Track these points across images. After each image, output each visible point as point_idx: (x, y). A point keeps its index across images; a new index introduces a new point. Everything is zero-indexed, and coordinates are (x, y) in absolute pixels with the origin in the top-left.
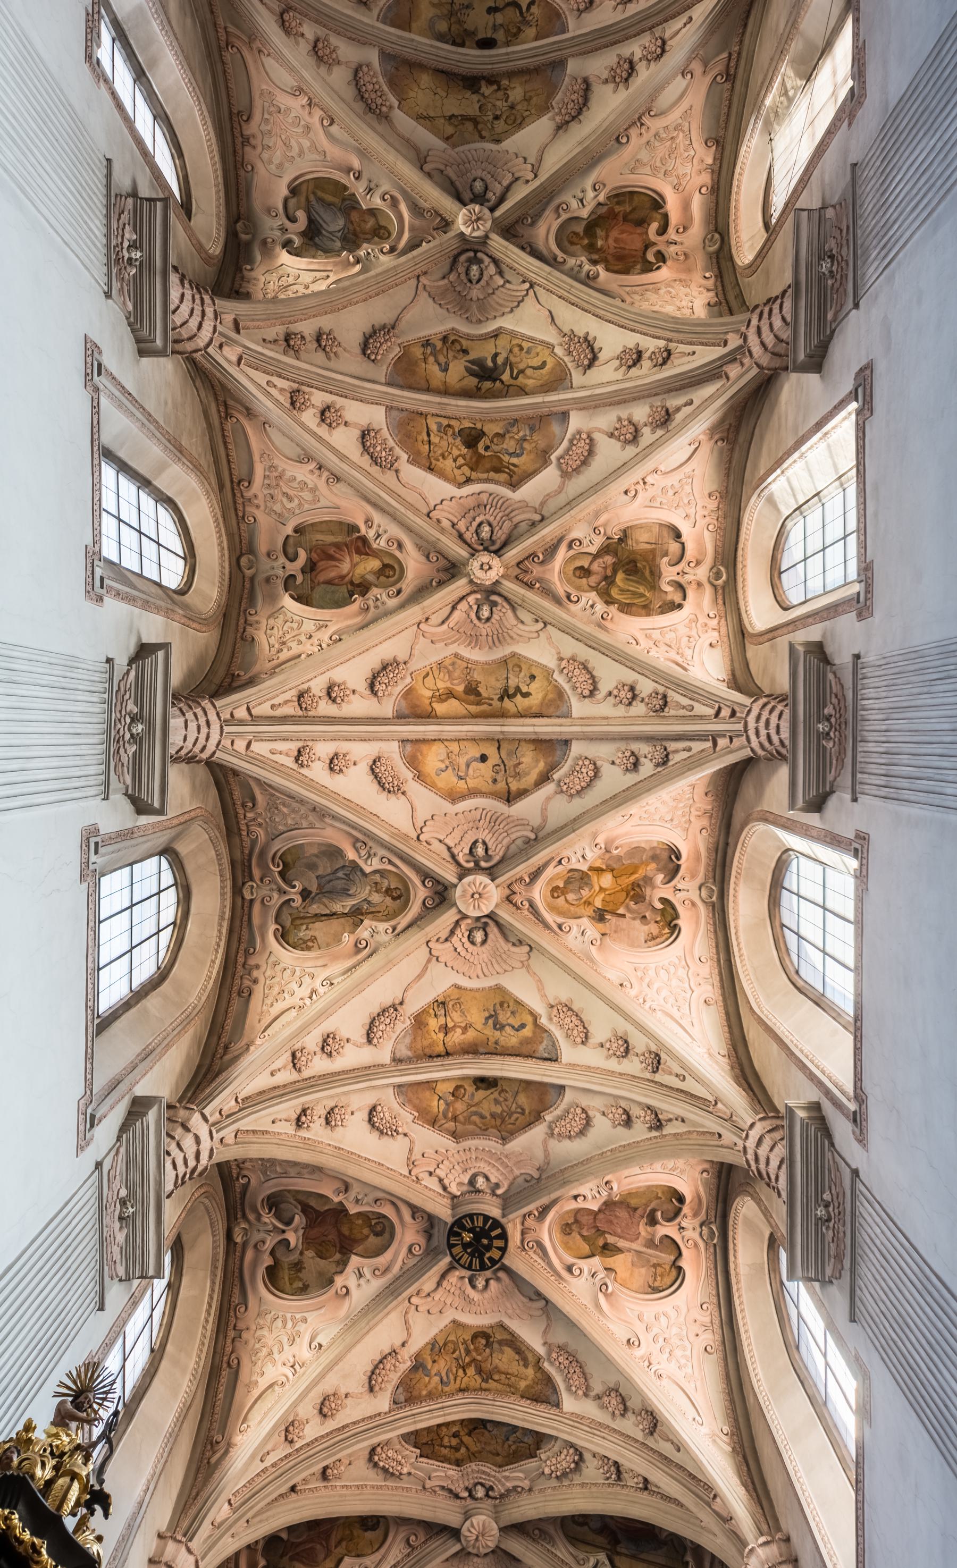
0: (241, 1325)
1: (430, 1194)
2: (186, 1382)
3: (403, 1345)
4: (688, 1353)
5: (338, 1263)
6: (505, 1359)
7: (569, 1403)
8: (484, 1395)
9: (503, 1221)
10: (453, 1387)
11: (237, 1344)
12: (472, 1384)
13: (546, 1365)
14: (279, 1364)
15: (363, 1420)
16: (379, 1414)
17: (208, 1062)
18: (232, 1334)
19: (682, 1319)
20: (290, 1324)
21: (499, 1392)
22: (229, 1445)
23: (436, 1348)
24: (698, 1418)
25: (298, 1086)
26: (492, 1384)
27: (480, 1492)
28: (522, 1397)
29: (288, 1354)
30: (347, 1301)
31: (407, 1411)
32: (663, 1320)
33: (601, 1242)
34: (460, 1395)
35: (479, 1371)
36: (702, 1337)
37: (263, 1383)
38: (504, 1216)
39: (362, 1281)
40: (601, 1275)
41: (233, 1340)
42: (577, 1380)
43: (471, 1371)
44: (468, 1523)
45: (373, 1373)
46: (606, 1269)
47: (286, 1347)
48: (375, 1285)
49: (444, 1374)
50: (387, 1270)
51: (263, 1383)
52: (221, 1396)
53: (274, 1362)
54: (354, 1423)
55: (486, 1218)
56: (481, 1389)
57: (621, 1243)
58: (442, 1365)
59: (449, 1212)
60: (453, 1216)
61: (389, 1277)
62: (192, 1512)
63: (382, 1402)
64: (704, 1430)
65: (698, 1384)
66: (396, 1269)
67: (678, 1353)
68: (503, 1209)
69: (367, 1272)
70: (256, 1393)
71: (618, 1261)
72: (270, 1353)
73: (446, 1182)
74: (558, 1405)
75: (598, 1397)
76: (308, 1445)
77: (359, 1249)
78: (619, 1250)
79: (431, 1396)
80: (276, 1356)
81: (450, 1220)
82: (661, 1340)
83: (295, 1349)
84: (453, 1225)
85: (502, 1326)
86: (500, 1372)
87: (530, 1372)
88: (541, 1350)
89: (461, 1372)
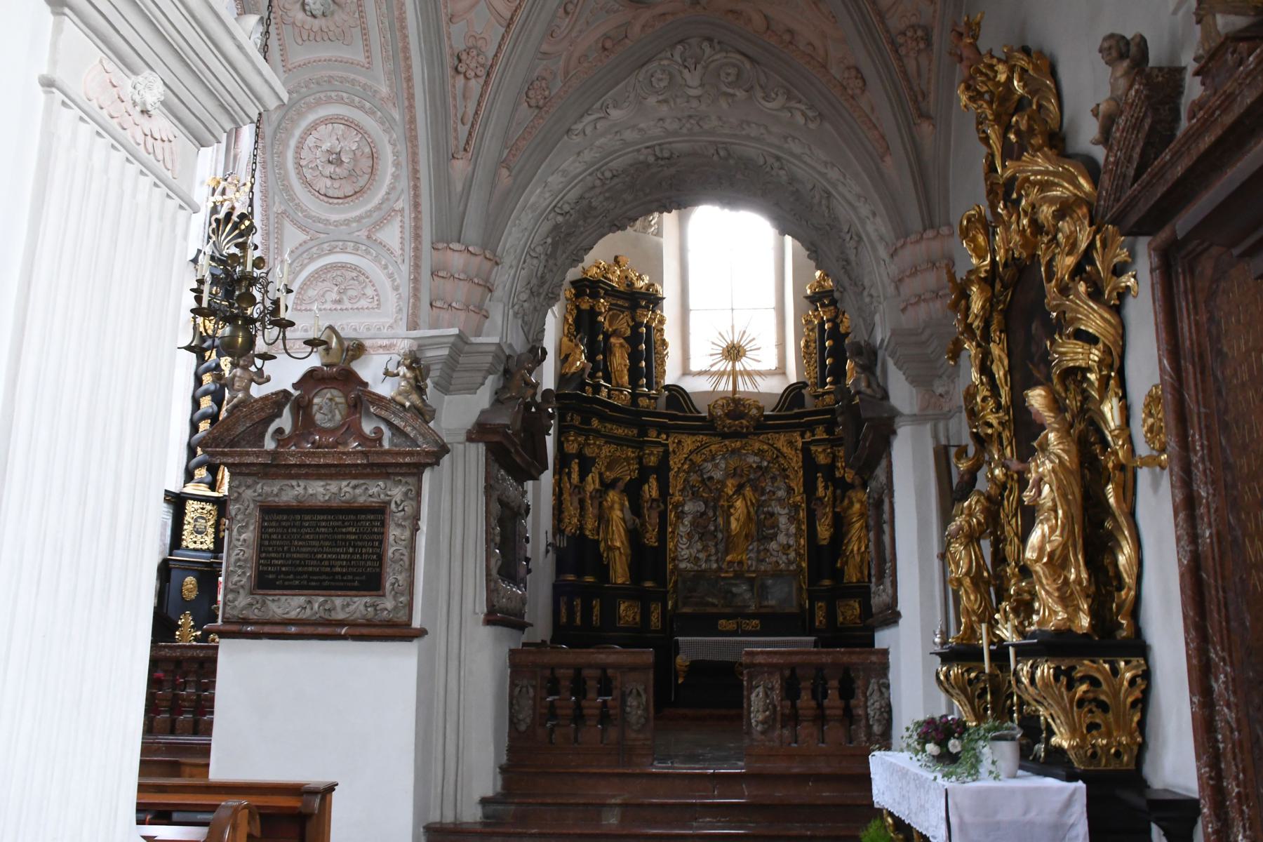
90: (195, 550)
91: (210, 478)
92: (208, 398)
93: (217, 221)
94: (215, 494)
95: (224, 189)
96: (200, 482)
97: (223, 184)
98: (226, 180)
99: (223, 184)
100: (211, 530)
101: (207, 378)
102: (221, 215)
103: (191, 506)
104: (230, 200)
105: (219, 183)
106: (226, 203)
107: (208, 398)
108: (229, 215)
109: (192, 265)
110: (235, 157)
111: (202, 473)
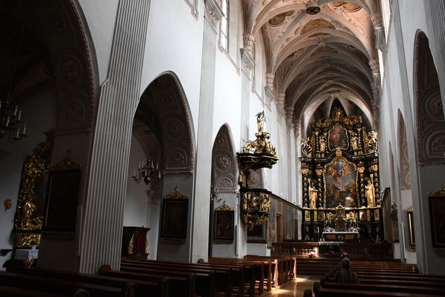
0: (266, 31)
1: (301, 5)
2: (261, 49)
3: (301, 26)
4: (363, 19)
5: (283, 18)
6: (323, 22)
7: (337, 29)
8: (319, 28)
9: (319, 7)
10: (312, 28)
11: (267, 35)
12: (317, 26)
13: (332, 24)
14: (276, 37)
15: (295, 39)
16: (298, 37)
17: (245, 12)
18: (265, 33)
19: (362, 13)
20: (276, 30)
21: (322, 27)
22: (272, 54)
23: (308, 24)
24: (364, 34)
25: (266, 9)
26: (320, 26)
27: (321, 39)
28: (327, 27)
29: (278, 35)
30: (287, 25)
31: (304, 35)
32: (357, 14)
33: (342, 2)
34: (314, 29)
35: (318, 24)
36: (366, 16)
37: (275, 41)
38: (318, 6)
39: (289, 20)
40: (343, 9)
41: (266, 34)
42: (339, 26)
43: (316, 24)
44: (319, 44)
45: (295, 32)
46: (344, 7)
47: (277, 34)
48: (292, 20)
49: (310, 27)
50: (294, 17)
51: (275, 41)
52: (267, 44)
53: (275, 36)
54: (294, 40)
55: (314, 7)
56: (319, 27)
57: (347, 2)
58: (310, 26)
59: (306, 7)
60: (307, 8)
61: (295, 18)
62: (269, 67)
63: (299, 35)
64: (365, 36)
65: (365, 25)
66: (296, 16)
67: (361, 20)
68: (318, 4)
69: (290, 18)
70: (274, 43)
71: (347, 5)
72: (274, 35)
73: (304, 2)
74: (335, 29)
75: (343, 28)
76: (286, 47)
77: (287, 14)
78: (347, 3)
79: (308, 31)
80: (275, 35)
81: (306, 9)
82: (357, 18)
83: (279, 34)
84: (307, 10)
85: (321, 18)
86: (322, 24)
87: (329, 24)
88: (330, 21)
89: (314, 25)
90: (307, 221)
91: (308, 206)
92: (306, 188)
93: (303, 148)
94: (309, 209)
95: (304, 141)
96: (306, 206)
97: (303, 140)
98: (304, 139)
99: (303, 140)
100: (310, 217)
101: (305, 184)
102: (304, 147)
103: (306, 212)
104: (305, 143)
105: (302, 140)
106: (305, 144)
107: (306, 188)
108: (306, 146)
109: (299, 159)
110: (304, 133)
111: (306, 204)
